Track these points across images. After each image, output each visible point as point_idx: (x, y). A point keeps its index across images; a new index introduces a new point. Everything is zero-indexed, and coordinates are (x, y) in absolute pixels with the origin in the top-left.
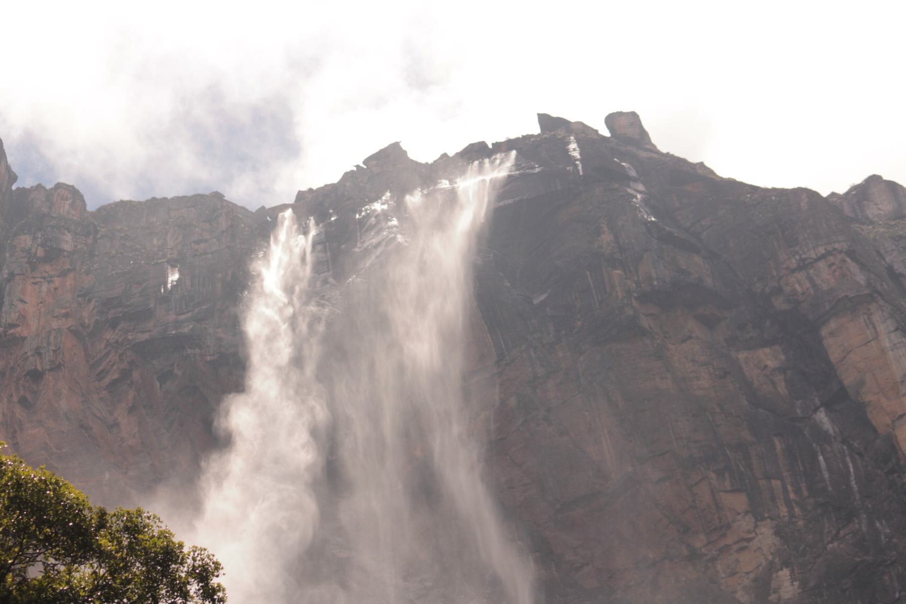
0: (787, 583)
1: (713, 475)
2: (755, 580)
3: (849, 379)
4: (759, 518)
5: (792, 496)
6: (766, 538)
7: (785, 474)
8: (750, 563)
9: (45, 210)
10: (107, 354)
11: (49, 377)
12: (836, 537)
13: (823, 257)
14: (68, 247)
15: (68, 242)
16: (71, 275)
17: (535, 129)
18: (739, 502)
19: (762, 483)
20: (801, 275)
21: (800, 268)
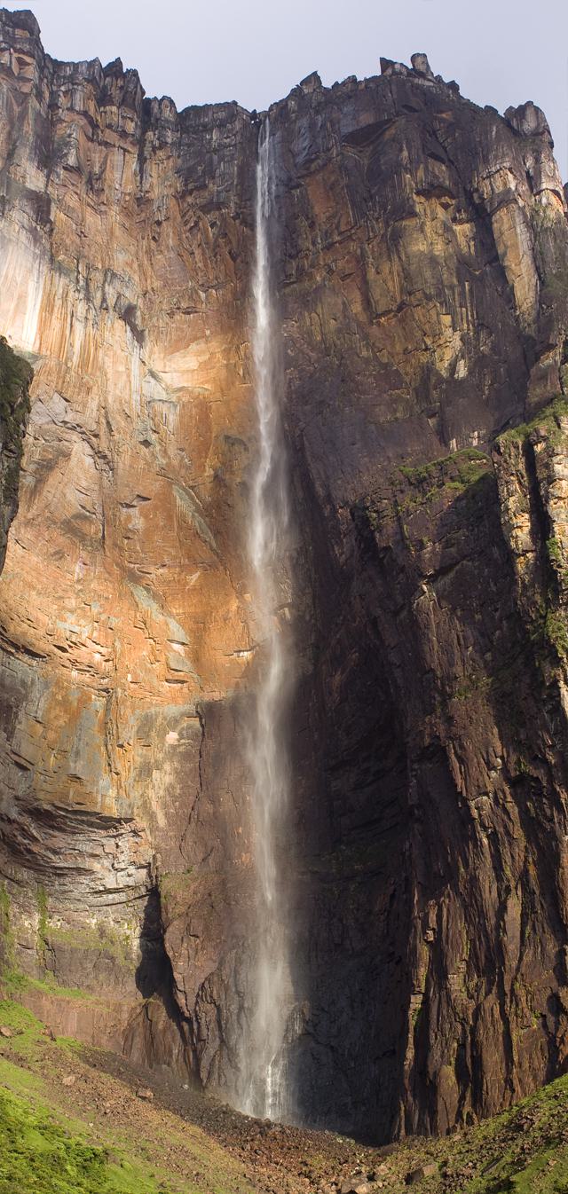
0: (462, 369)
1: (439, 305)
2: (450, 365)
3: (500, 250)
4: (455, 330)
5: (470, 318)
6: (457, 343)
7: (468, 305)
8: (449, 355)
9: (158, 116)
10: (188, 211)
11: (164, 224)
12: (485, 344)
13: (498, 171)
14: (169, 140)
15: (170, 137)
16: (171, 159)
17: (378, 73)
18: (447, 320)
19: (458, 309)
20: (487, 182)
21: (487, 177)
